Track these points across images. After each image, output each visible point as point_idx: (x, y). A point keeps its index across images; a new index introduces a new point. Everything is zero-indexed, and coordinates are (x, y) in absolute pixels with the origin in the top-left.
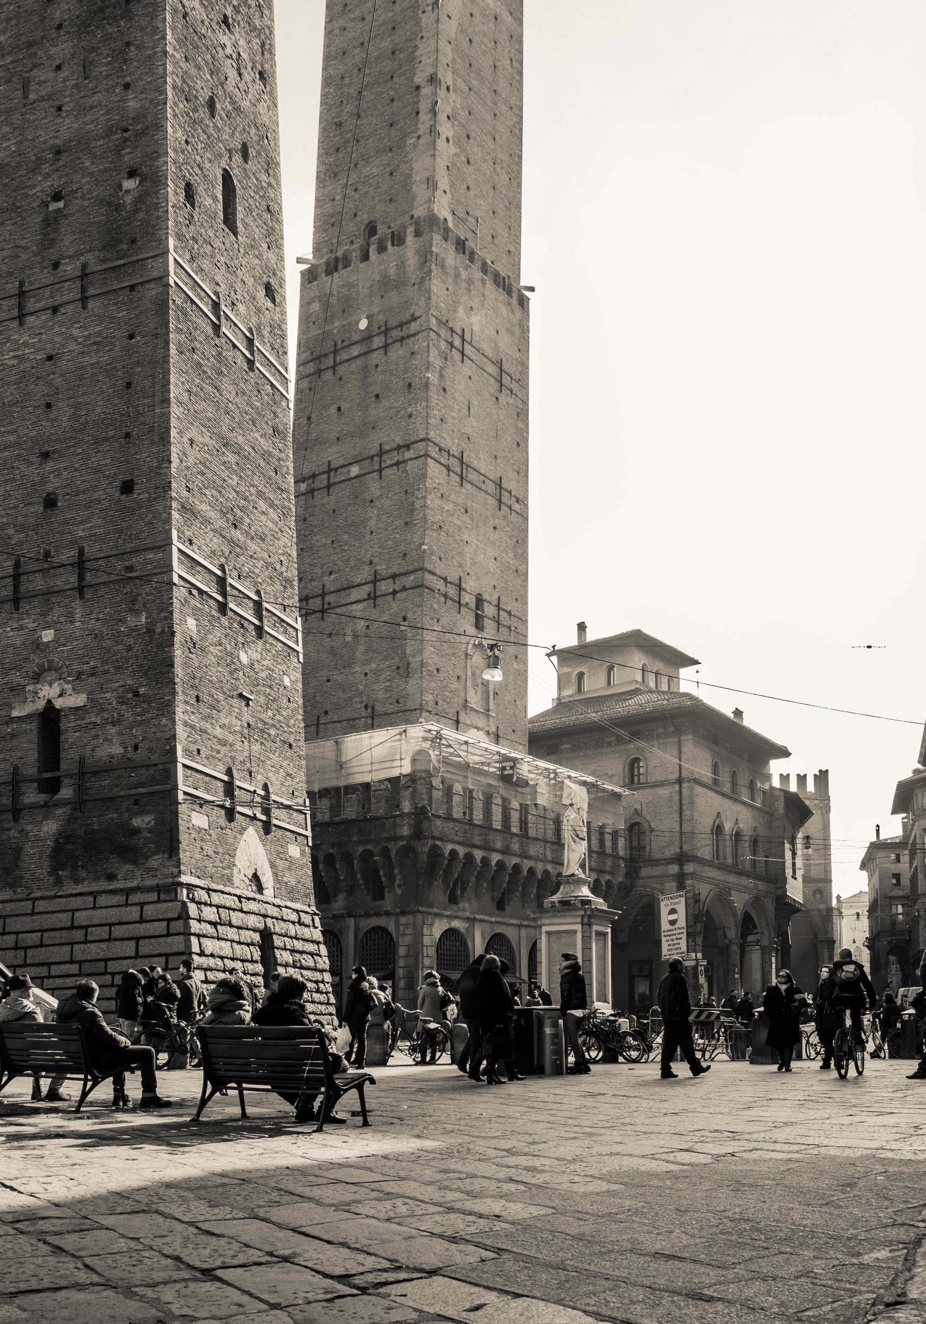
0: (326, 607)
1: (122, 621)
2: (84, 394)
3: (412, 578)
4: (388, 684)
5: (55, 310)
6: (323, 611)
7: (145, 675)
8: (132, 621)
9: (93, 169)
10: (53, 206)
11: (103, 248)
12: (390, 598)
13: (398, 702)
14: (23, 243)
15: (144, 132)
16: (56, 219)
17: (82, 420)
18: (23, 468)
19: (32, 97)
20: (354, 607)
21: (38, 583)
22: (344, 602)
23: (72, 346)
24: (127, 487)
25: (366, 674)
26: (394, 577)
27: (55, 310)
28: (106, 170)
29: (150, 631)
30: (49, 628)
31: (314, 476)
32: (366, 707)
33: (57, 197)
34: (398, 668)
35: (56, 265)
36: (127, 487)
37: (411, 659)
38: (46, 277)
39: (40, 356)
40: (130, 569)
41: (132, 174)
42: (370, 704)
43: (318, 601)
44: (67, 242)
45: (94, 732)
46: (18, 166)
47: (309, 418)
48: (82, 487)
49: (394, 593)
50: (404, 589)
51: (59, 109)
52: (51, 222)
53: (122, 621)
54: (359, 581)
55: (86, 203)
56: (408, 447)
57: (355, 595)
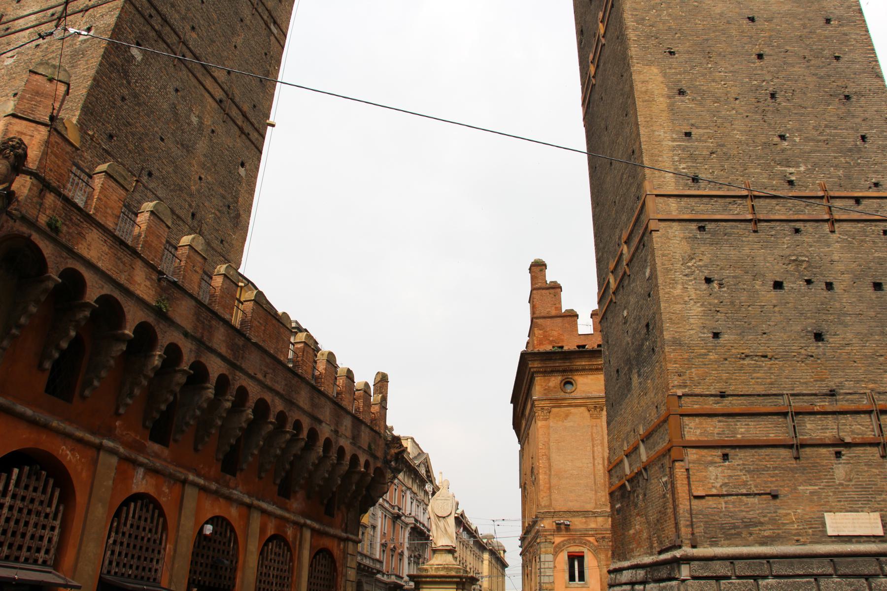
3: (256, 135)
4: (217, 213)
12: (238, 133)
13: (222, 241)
20: (207, 95)
22: (199, 75)
25: (200, 178)
26: (244, 115)
32: (193, 215)
34: (229, 207)
37: (241, 212)
42: (198, 216)
49: (241, 129)
50: (247, 135)
54: (215, 74)
56: (275, 23)
57: (209, 82)
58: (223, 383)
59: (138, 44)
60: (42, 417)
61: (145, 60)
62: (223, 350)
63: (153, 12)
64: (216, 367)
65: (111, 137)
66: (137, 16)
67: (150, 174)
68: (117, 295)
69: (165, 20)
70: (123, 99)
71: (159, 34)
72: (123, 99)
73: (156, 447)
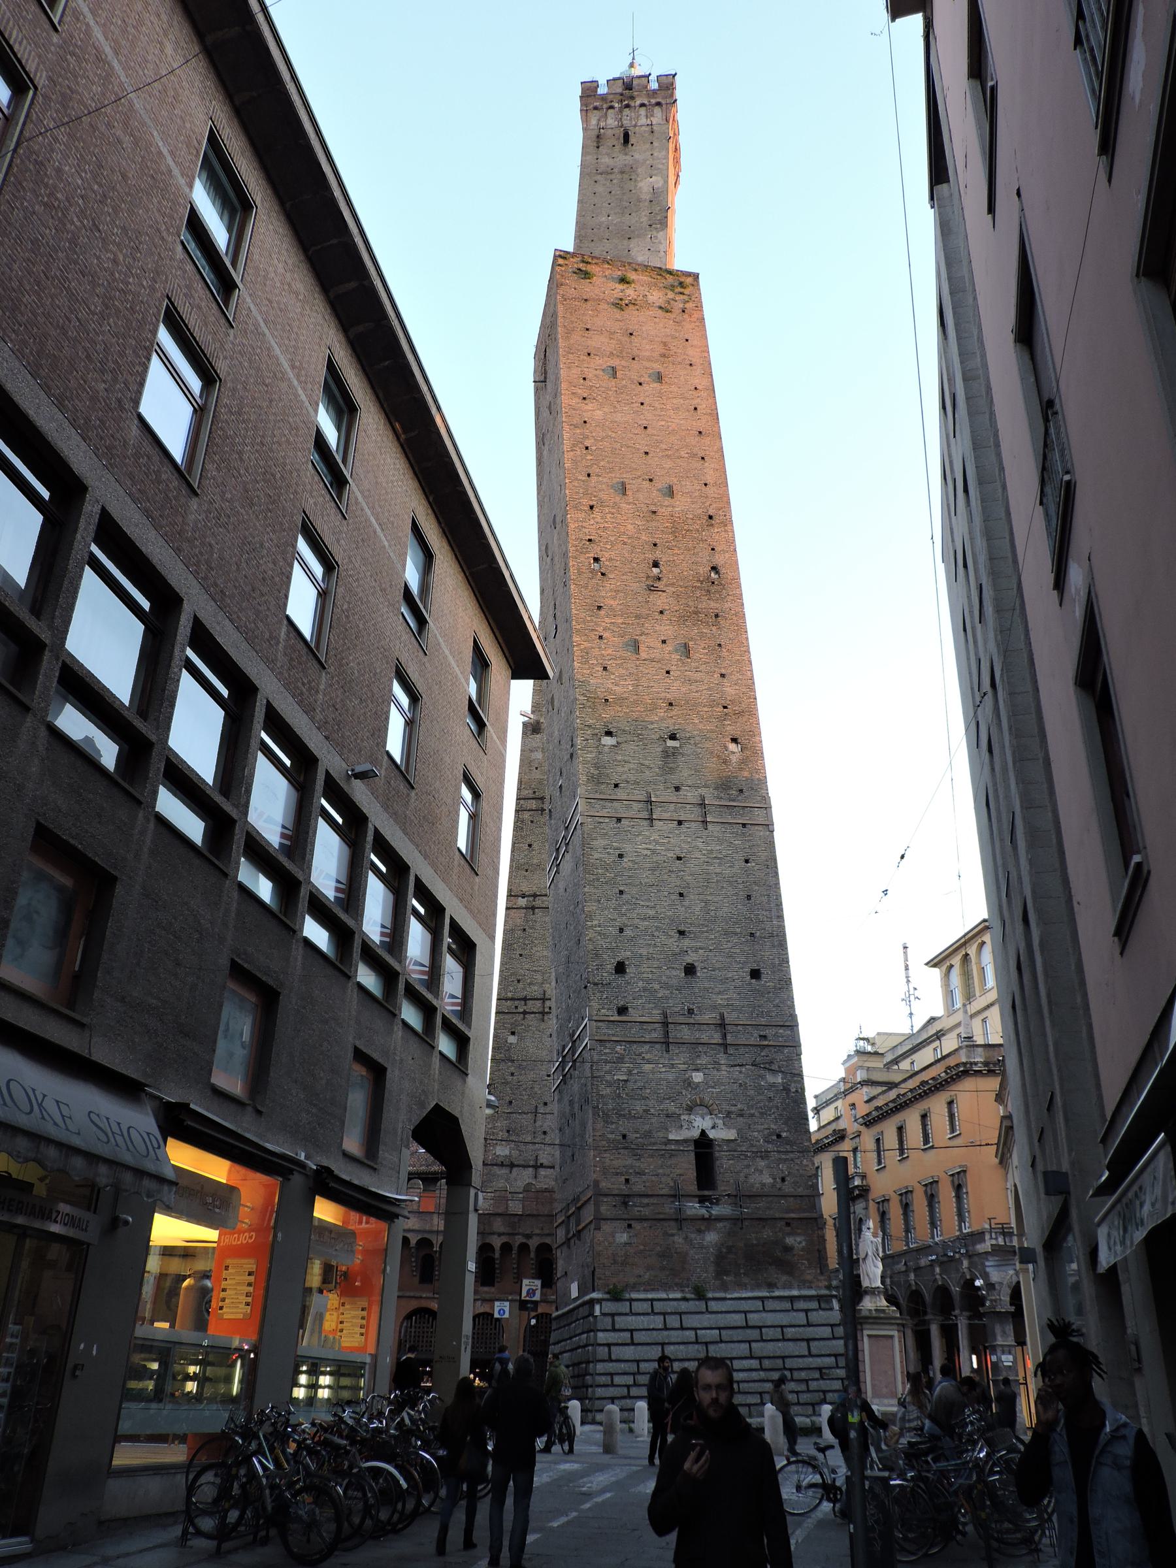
0: (547, 1010)
1: (763, 1077)
2: (711, 894)
5: (680, 823)
6: (543, 1013)
7: (785, 1123)
8: (770, 1078)
9: (701, 726)
10: (670, 743)
11: (716, 789)
14: (647, 762)
15: (740, 714)
16: (674, 754)
17: (712, 913)
18: (663, 938)
19: (643, 655)
21: (685, 1034)
23: (698, 855)
24: (755, 974)
27: (680, 823)
28: (712, 731)
29: (786, 1089)
30: (697, 1070)
31: (535, 896)
33: (673, 737)
35: (677, 789)
36: (755, 974)
38: (670, 796)
39: (671, 854)
40: (764, 1037)
41: (734, 740)
43: (539, 1003)
44: (684, 774)
45: (746, 1162)
46: (636, 702)
47: (530, 846)
48: (717, 965)
51: (668, 672)
52: (668, 754)
53: (763, 1077)
55: (699, 750)
58: (506, 1247)
59: (513, 1033)
60: (418, 1294)
61: (521, 1039)
62: (502, 1230)
63: (517, 1003)
64: (497, 1242)
65: (511, 1102)
66: (506, 1016)
67: (546, 1104)
68: (426, 1236)
69: (525, 999)
70: (512, 1074)
71: (525, 1013)
72: (512, 1074)
73: (486, 1289)
